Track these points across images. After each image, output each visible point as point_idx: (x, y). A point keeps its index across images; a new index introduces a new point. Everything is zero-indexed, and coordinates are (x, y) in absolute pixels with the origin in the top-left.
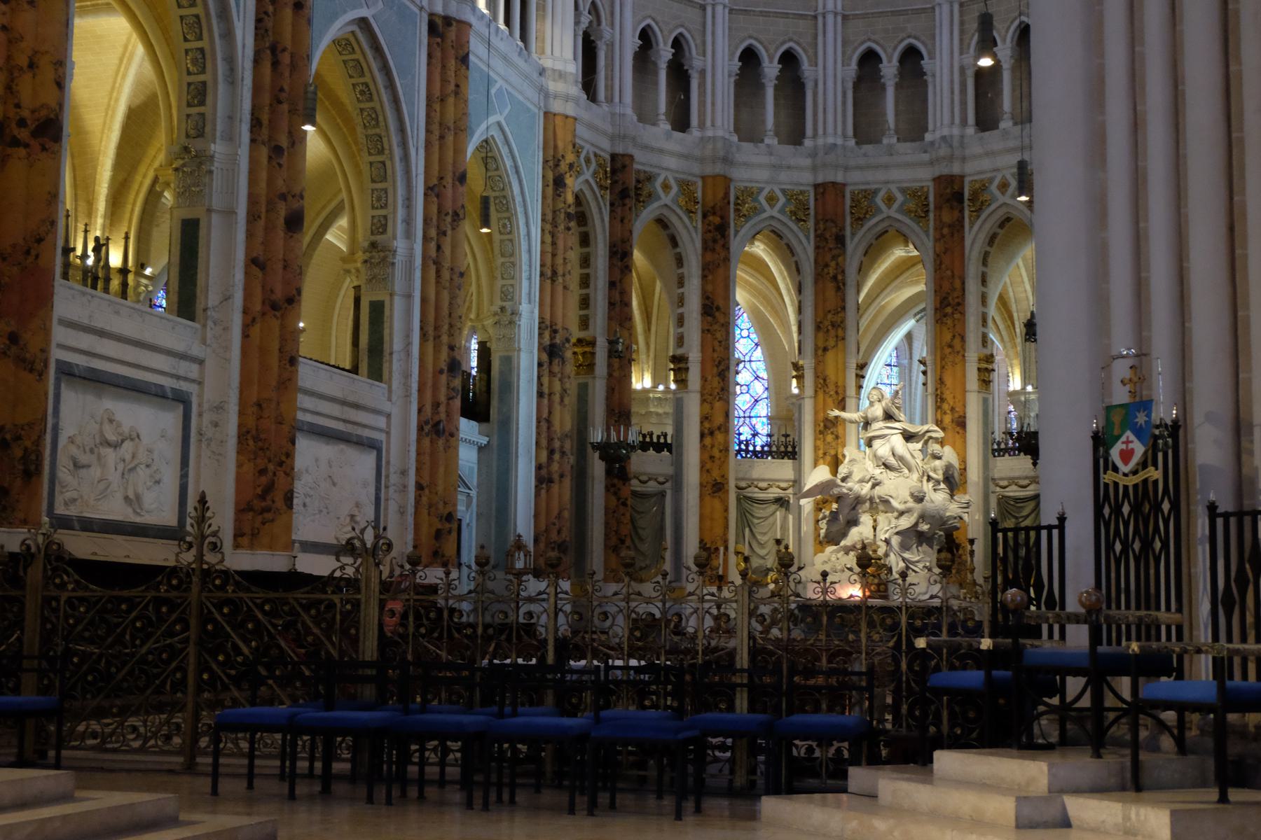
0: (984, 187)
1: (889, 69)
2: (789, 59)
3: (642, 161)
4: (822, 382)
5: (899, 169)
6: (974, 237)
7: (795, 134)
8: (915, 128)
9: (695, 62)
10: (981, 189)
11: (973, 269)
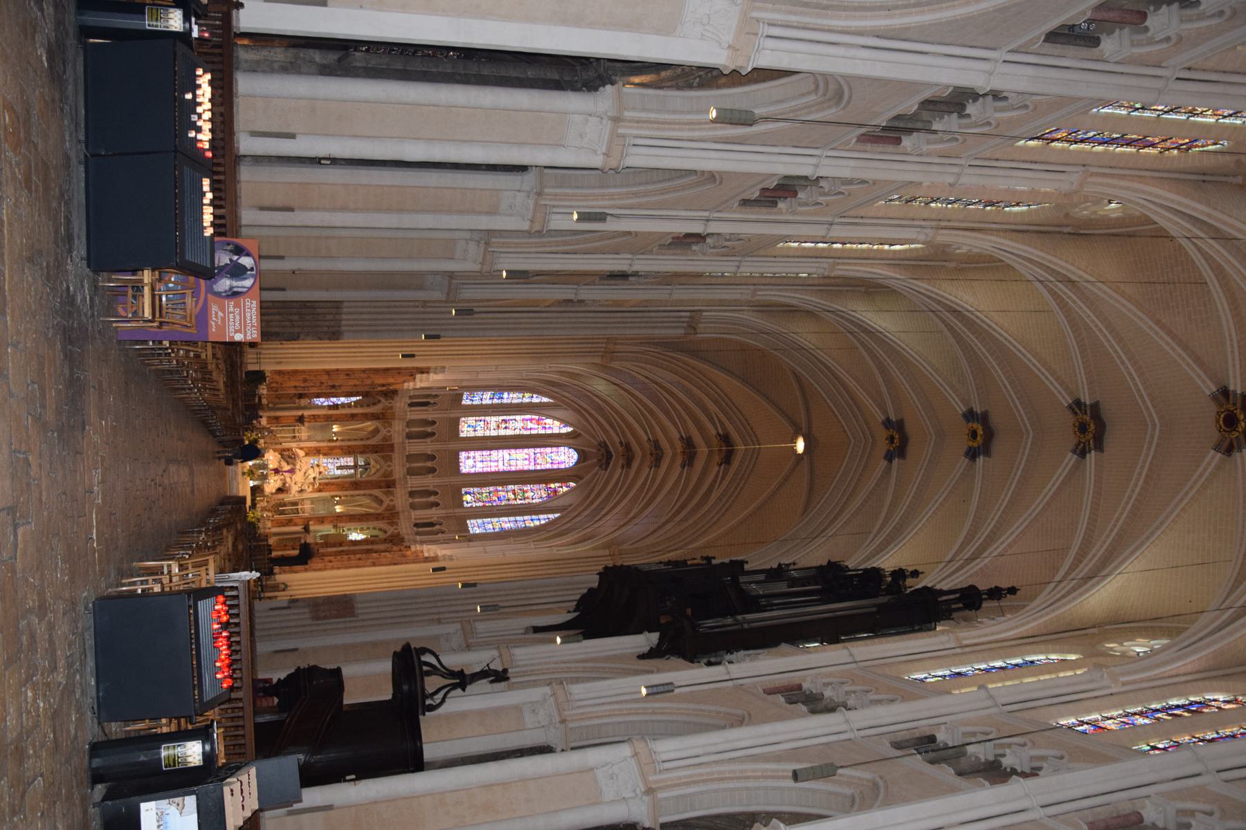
0: (392, 494)
1: (429, 464)
2: (433, 434)
3: (397, 398)
4: (332, 448)
5: (398, 468)
6: (376, 492)
7: (410, 436)
8: (411, 472)
9: (430, 408)
10: (392, 494)
11: (368, 492)
